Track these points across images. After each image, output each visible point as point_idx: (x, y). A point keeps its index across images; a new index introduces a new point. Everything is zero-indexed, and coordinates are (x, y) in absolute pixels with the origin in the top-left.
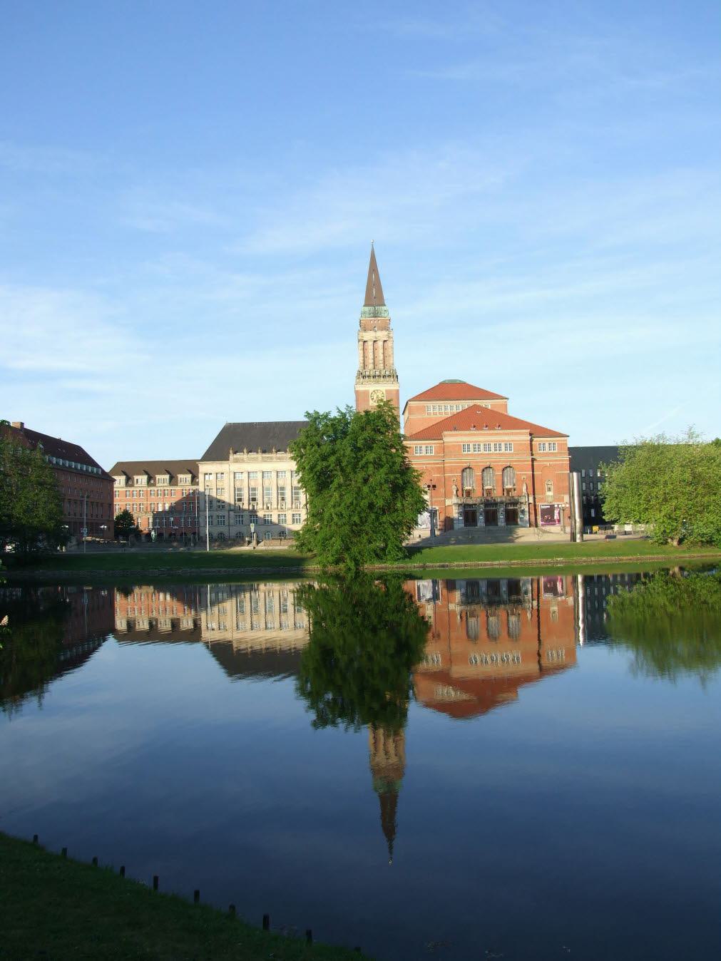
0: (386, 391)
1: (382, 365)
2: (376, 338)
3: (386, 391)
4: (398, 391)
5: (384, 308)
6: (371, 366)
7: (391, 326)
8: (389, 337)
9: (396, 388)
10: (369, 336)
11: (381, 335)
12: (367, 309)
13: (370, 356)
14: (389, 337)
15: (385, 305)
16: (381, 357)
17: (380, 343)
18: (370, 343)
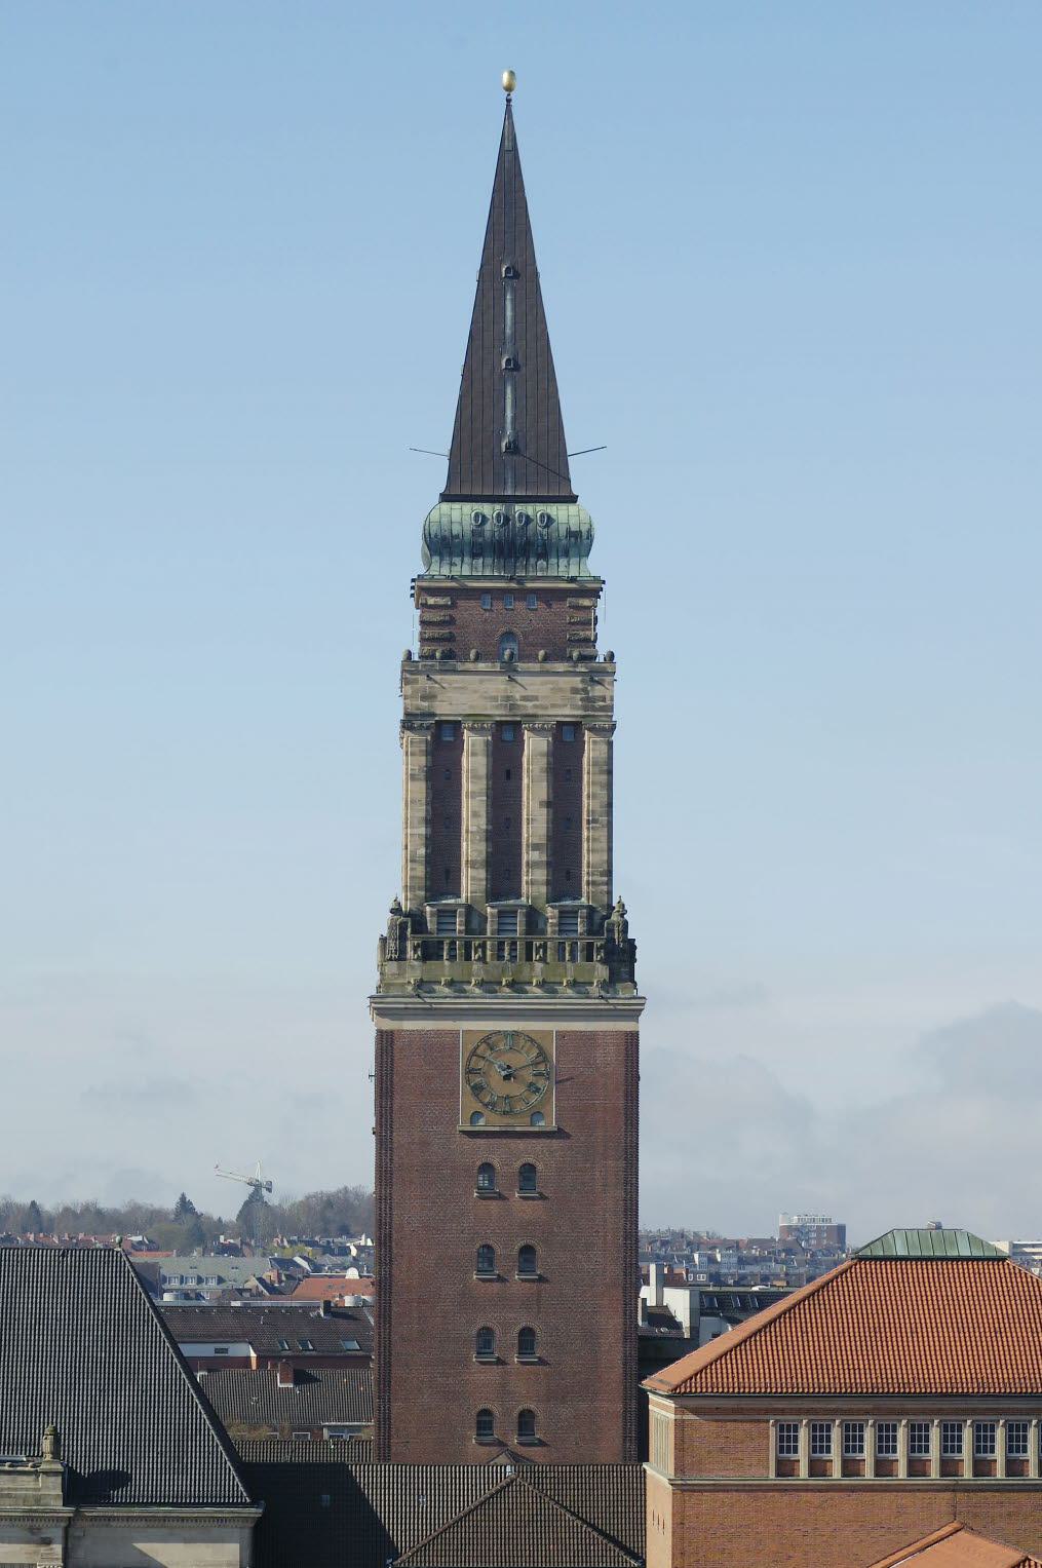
2: (513, 707)
3: (561, 1035)
4: (632, 1039)
5: (559, 512)
8: (589, 701)
9: (625, 1026)
10: (471, 693)
12: (462, 515)
14: (589, 701)
17: (534, 748)
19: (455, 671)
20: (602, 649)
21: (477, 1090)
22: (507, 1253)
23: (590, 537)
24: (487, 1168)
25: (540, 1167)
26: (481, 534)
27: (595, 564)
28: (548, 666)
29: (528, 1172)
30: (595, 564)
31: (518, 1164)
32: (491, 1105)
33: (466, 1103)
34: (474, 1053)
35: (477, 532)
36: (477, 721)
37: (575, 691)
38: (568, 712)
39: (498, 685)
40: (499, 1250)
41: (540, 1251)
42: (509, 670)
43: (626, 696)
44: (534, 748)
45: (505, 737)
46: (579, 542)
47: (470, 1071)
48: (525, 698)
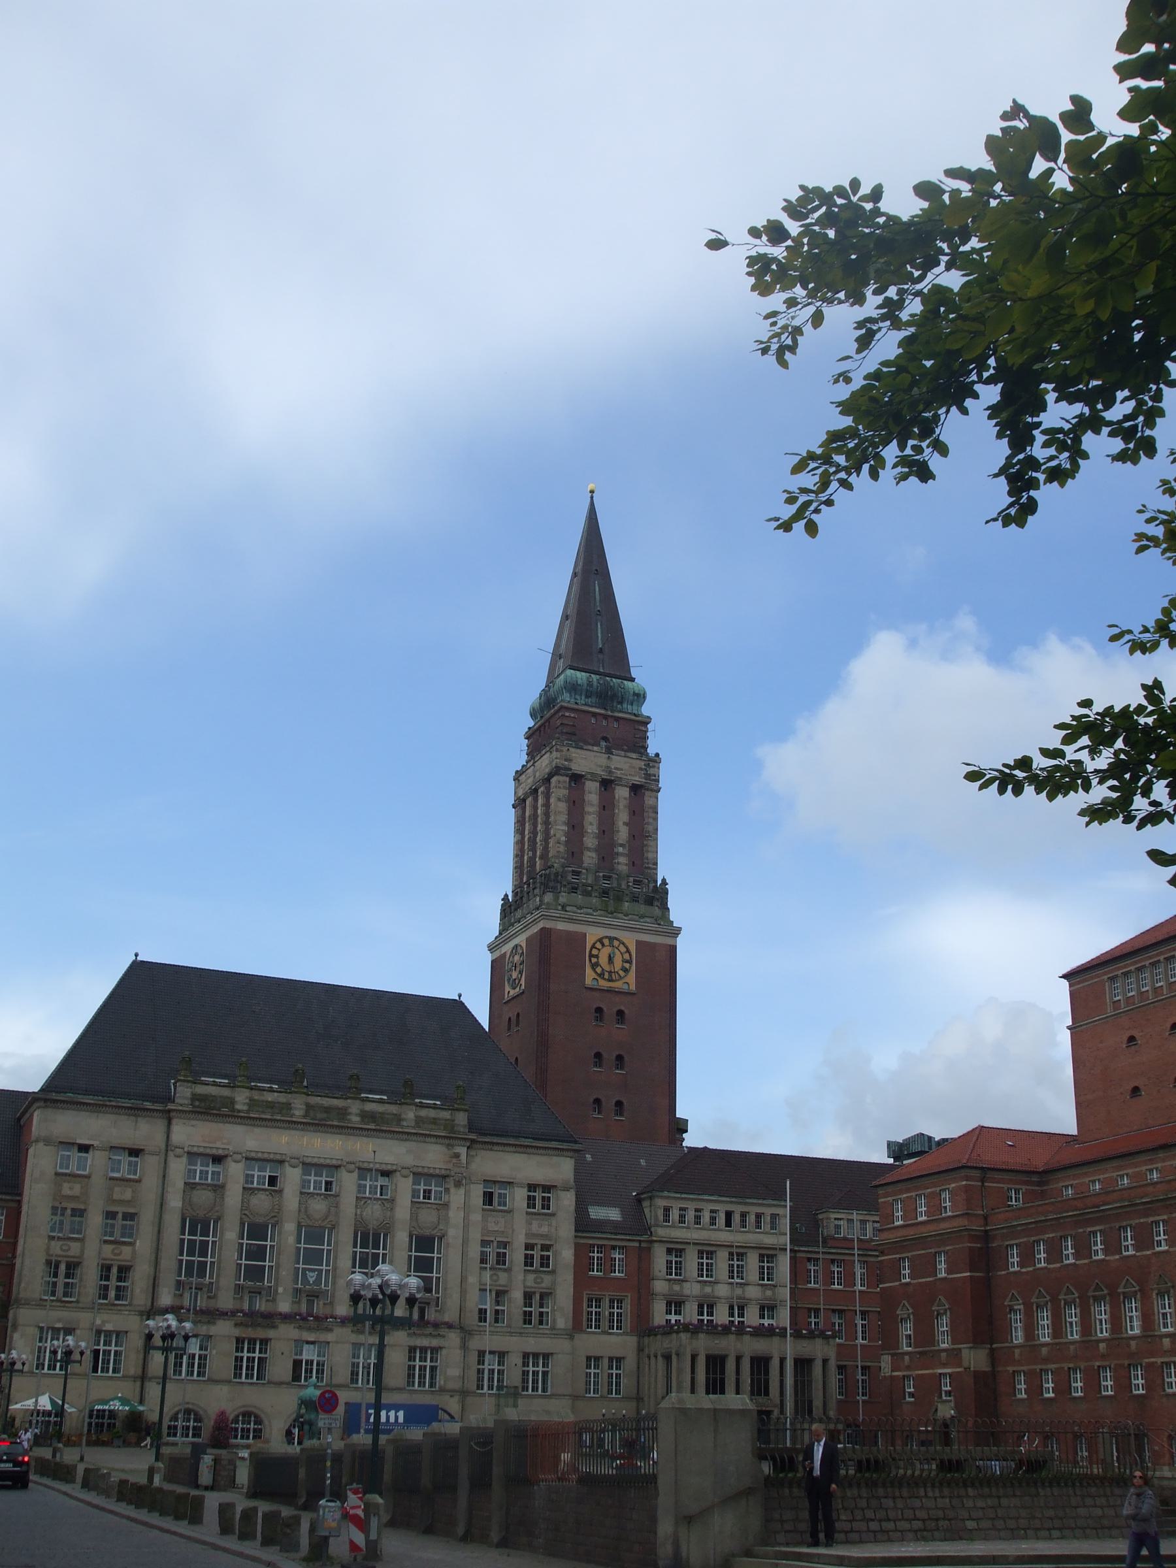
0: (638, 943)
1: (622, 860)
2: (610, 772)
3: (638, 943)
4: (673, 950)
6: (590, 859)
7: (653, 746)
8: (647, 776)
9: (669, 941)
11: (624, 765)
12: (581, 677)
13: (591, 825)
14: (647, 776)
15: (633, 680)
16: (623, 834)
17: (622, 793)
18: (592, 787)
19: (582, 748)
20: (651, 751)
21: (594, 966)
22: (609, 1056)
23: (644, 697)
24: (599, 1010)
25: (626, 1012)
26: (591, 686)
27: (646, 710)
28: (629, 754)
29: (620, 1013)
30: (646, 710)
31: (615, 1010)
32: (601, 975)
33: (589, 976)
34: (593, 947)
35: (590, 684)
36: (593, 776)
37: (641, 769)
38: (638, 779)
39: (602, 759)
40: (605, 1055)
41: (626, 1059)
42: (609, 751)
43: (666, 775)
44: (622, 793)
45: (607, 784)
46: (640, 697)
47: (591, 956)
48: (616, 768)
